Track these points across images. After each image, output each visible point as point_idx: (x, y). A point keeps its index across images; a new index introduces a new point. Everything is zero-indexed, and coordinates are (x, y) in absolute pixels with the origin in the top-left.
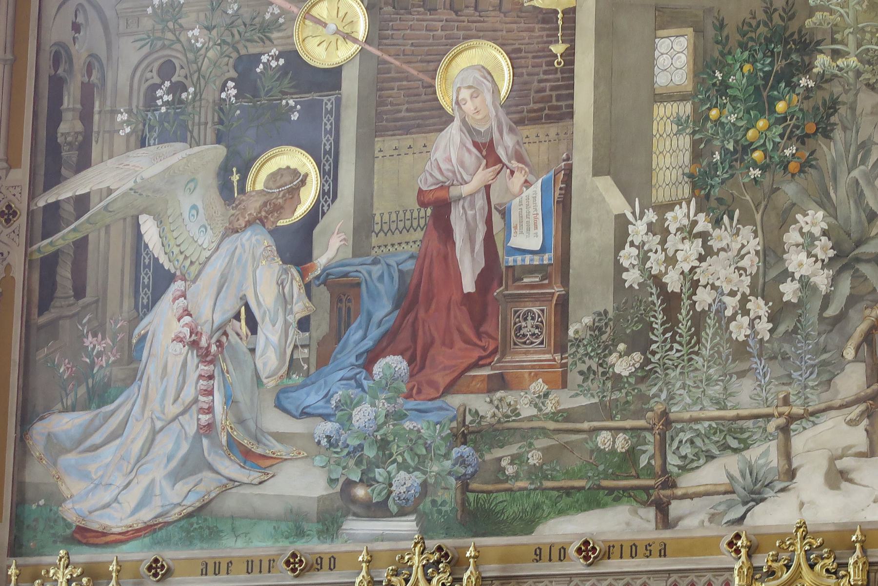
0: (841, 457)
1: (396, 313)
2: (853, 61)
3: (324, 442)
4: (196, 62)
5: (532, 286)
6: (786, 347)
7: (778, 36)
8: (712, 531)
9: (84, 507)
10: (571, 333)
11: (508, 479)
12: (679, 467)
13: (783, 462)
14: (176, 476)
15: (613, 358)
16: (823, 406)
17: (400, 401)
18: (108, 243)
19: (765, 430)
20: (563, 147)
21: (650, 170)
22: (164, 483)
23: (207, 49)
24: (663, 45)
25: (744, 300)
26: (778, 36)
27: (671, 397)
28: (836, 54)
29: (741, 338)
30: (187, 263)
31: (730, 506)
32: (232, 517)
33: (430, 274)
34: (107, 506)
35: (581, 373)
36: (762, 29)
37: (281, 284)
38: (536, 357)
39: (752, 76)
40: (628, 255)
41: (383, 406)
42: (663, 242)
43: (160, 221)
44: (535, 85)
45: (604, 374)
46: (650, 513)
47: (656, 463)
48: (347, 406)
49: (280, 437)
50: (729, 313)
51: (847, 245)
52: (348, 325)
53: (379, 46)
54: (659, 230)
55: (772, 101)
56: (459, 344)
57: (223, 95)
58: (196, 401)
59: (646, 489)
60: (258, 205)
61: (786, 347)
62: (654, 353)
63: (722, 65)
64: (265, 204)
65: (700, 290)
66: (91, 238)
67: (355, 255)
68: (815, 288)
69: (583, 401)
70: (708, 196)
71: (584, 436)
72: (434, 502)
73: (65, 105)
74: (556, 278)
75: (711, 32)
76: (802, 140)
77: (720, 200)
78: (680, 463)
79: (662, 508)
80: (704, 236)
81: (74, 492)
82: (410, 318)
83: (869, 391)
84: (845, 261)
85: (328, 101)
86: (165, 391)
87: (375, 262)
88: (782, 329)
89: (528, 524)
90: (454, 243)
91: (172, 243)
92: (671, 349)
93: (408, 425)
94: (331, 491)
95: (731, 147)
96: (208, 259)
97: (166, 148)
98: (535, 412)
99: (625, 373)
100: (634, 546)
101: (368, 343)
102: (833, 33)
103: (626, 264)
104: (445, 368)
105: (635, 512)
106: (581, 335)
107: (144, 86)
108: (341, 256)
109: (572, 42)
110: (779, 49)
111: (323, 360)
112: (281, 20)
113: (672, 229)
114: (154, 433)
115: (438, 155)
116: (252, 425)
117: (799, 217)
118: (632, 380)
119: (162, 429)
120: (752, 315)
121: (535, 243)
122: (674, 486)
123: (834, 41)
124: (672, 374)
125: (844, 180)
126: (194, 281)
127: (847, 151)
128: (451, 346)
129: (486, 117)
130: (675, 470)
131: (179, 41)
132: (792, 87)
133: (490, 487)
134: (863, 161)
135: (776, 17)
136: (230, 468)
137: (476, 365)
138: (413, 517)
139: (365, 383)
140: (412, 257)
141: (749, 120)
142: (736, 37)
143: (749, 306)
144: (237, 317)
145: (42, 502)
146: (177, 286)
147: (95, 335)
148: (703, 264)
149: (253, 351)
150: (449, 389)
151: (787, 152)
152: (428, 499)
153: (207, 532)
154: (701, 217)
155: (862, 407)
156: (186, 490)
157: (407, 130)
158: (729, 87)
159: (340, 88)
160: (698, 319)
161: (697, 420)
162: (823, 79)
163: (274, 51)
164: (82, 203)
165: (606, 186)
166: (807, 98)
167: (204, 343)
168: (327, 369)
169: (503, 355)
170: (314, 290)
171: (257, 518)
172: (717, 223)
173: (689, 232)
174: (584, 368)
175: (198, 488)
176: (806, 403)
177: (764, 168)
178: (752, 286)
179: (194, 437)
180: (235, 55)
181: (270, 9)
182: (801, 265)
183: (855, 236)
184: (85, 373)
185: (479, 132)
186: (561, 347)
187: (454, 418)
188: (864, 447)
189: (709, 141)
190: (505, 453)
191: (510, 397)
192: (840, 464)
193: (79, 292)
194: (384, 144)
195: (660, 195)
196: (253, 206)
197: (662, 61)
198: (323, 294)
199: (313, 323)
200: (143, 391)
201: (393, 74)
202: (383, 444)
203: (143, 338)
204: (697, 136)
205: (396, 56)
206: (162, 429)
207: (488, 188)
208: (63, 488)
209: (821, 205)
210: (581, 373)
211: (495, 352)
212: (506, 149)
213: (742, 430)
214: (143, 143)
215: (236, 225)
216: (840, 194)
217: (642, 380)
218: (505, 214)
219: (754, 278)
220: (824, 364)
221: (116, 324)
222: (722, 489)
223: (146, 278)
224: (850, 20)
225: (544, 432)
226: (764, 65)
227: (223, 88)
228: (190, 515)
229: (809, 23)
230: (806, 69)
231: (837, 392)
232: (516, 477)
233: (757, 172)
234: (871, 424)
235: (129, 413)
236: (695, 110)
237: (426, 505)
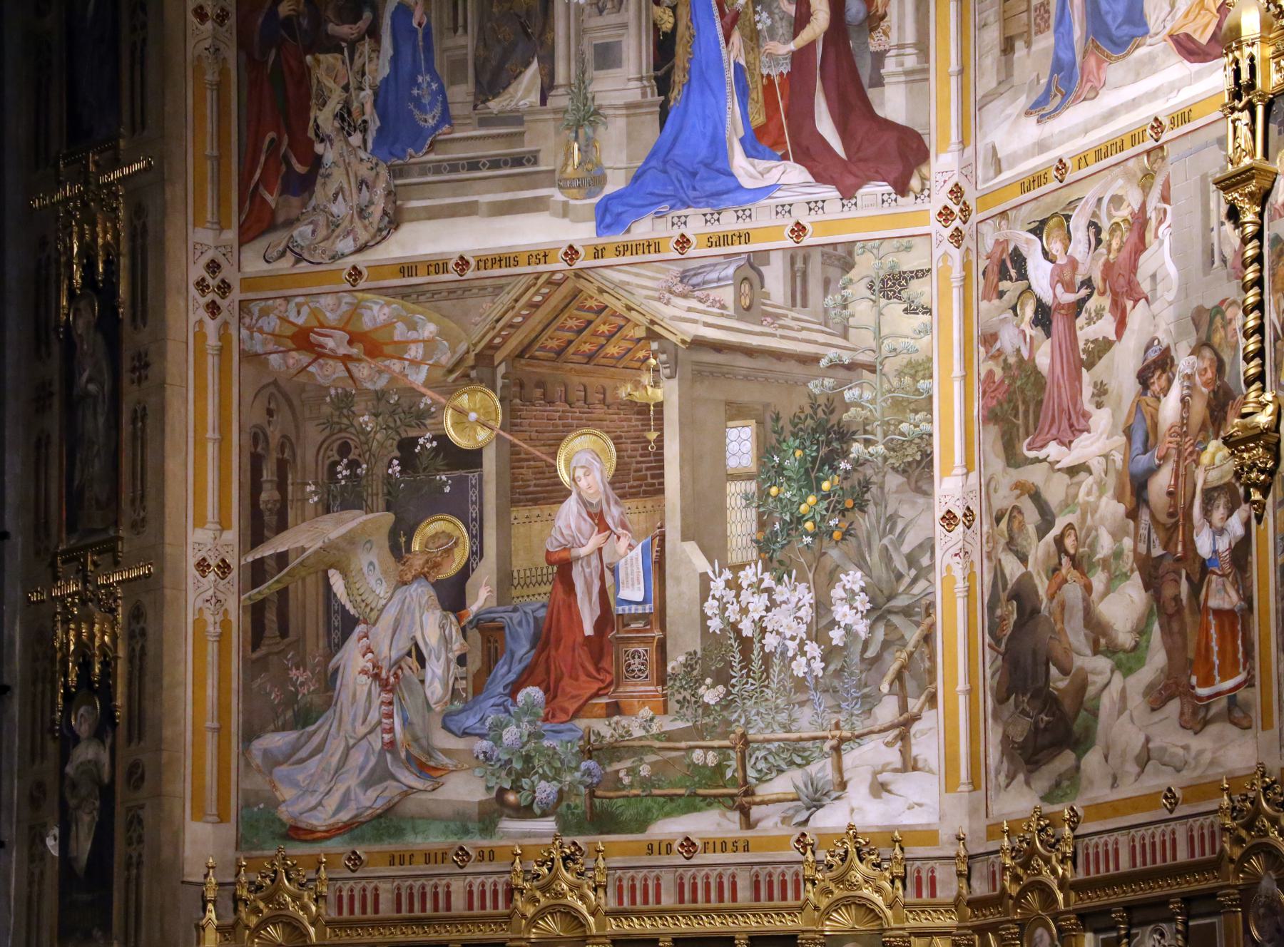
0: (881, 773)
1: (533, 652)
2: (880, 449)
3: (481, 757)
4: (366, 443)
5: (638, 631)
6: (836, 683)
7: (821, 427)
8: (784, 830)
9: (296, 809)
10: (669, 669)
11: (625, 787)
12: (757, 779)
13: (837, 776)
14: (367, 784)
15: (702, 690)
16: (866, 730)
17: (539, 723)
18: (304, 592)
19: (822, 750)
20: (657, 517)
21: (725, 537)
22: (358, 790)
23: (376, 433)
24: (732, 434)
25: (802, 644)
26: (821, 427)
27: (748, 722)
28: (868, 443)
29: (801, 675)
30: (368, 610)
31: (797, 811)
32: (412, 818)
33: (558, 620)
34: (314, 808)
35: (678, 702)
36: (809, 421)
37: (442, 627)
38: (643, 688)
39: (803, 461)
40: (711, 606)
41: (526, 728)
42: (737, 596)
43: (345, 576)
44: (634, 466)
45: (696, 702)
46: (736, 816)
47: (739, 775)
48: (499, 727)
49: (447, 752)
50: (790, 654)
51: (881, 600)
52: (496, 661)
53: (511, 432)
54: (734, 585)
55: (819, 481)
56: (583, 678)
57: (390, 471)
58: (380, 723)
59: (732, 796)
60: (421, 562)
61: (836, 683)
62: (733, 686)
63: (779, 451)
64: (427, 562)
65: (767, 635)
66: (291, 587)
67: (499, 605)
68: (856, 635)
69: (681, 725)
70: (771, 559)
71: (682, 753)
72: (568, 806)
73: (265, 477)
74: (656, 625)
75: (769, 423)
76: (843, 513)
77: (781, 562)
78: (755, 775)
79: (745, 812)
80: (769, 591)
81: (287, 797)
82: (544, 656)
83: (901, 719)
84: (879, 613)
85: (473, 477)
86: (355, 715)
87: (515, 610)
88: (832, 668)
89: (642, 824)
90: (575, 595)
91: (355, 592)
92: (747, 683)
93: (546, 743)
94: (488, 797)
95: (787, 518)
96: (385, 606)
97: (347, 514)
98: (643, 733)
99: (712, 702)
100: (724, 843)
101: (512, 677)
102: (865, 425)
103: (709, 613)
104: (573, 697)
105: (724, 815)
106: (677, 671)
107: (327, 462)
108: (488, 605)
109: (661, 430)
110: (823, 438)
111: (478, 689)
112: (433, 409)
113: (745, 585)
114: (348, 749)
115: (560, 523)
116: (424, 742)
117: (842, 576)
118: (718, 708)
119: (354, 745)
120: (809, 656)
121: (639, 596)
122: (753, 794)
123: (866, 432)
124: (749, 703)
125: (876, 546)
126: (374, 624)
127: (878, 522)
128: (577, 679)
129: (597, 492)
130: (754, 781)
131: (352, 425)
132: (834, 469)
133: (611, 794)
134: (892, 530)
135: (820, 411)
136: (409, 779)
137: (596, 695)
138: (553, 818)
139: (511, 709)
140: (543, 606)
141: (801, 497)
142: (789, 428)
143: (806, 648)
144: (409, 654)
145: (262, 806)
146: (360, 628)
147: (298, 669)
148: (770, 614)
149: (422, 682)
150: (576, 715)
151: (832, 523)
152: (564, 804)
153: (392, 831)
154: (767, 576)
155: (896, 732)
156: (375, 795)
157: (535, 502)
158: (784, 469)
159: (481, 466)
160: (767, 658)
161: (769, 741)
162: (858, 463)
163: (428, 435)
164: (282, 559)
165: (692, 549)
166: (846, 479)
167: (384, 675)
168: (482, 697)
169: (618, 686)
170: (469, 633)
171: (432, 818)
172: (779, 580)
173: (758, 588)
174: (680, 697)
175: (385, 794)
176: (852, 728)
177: (814, 536)
178: (808, 632)
179: (380, 753)
180: (397, 438)
181: (424, 400)
182: (845, 615)
183: (886, 592)
184: (291, 699)
185: (591, 504)
186: (662, 680)
187: (581, 738)
188: (899, 765)
189: (770, 514)
190: (622, 766)
191: (624, 721)
192: (881, 778)
193: (284, 632)
194: (519, 513)
195: (734, 558)
196: (418, 563)
197: (732, 447)
198: (475, 635)
199: (469, 660)
200: (337, 715)
201: (523, 456)
202: (528, 759)
203: (336, 670)
204: (761, 510)
205: (524, 440)
206: (354, 745)
207: (600, 550)
208: (278, 794)
209: (860, 568)
210: (678, 702)
211: (610, 684)
212: (613, 518)
213: (804, 750)
214: (328, 510)
215: (405, 578)
216: (874, 559)
217: (725, 707)
218: (615, 571)
219: (809, 626)
220: (865, 696)
221: (314, 658)
222: (790, 797)
223: (336, 622)
224: (878, 415)
225: (651, 749)
226: (811, 451)
227: (390, 465)
228: (379, 816)
229: (845, 417)
230: (845, 454)
231: (876, 719)
232: (631, 786)
233: (809, 539)
234: (903, 746)
235: (328, 732)
236: (759, 488)
237: (563, 808)
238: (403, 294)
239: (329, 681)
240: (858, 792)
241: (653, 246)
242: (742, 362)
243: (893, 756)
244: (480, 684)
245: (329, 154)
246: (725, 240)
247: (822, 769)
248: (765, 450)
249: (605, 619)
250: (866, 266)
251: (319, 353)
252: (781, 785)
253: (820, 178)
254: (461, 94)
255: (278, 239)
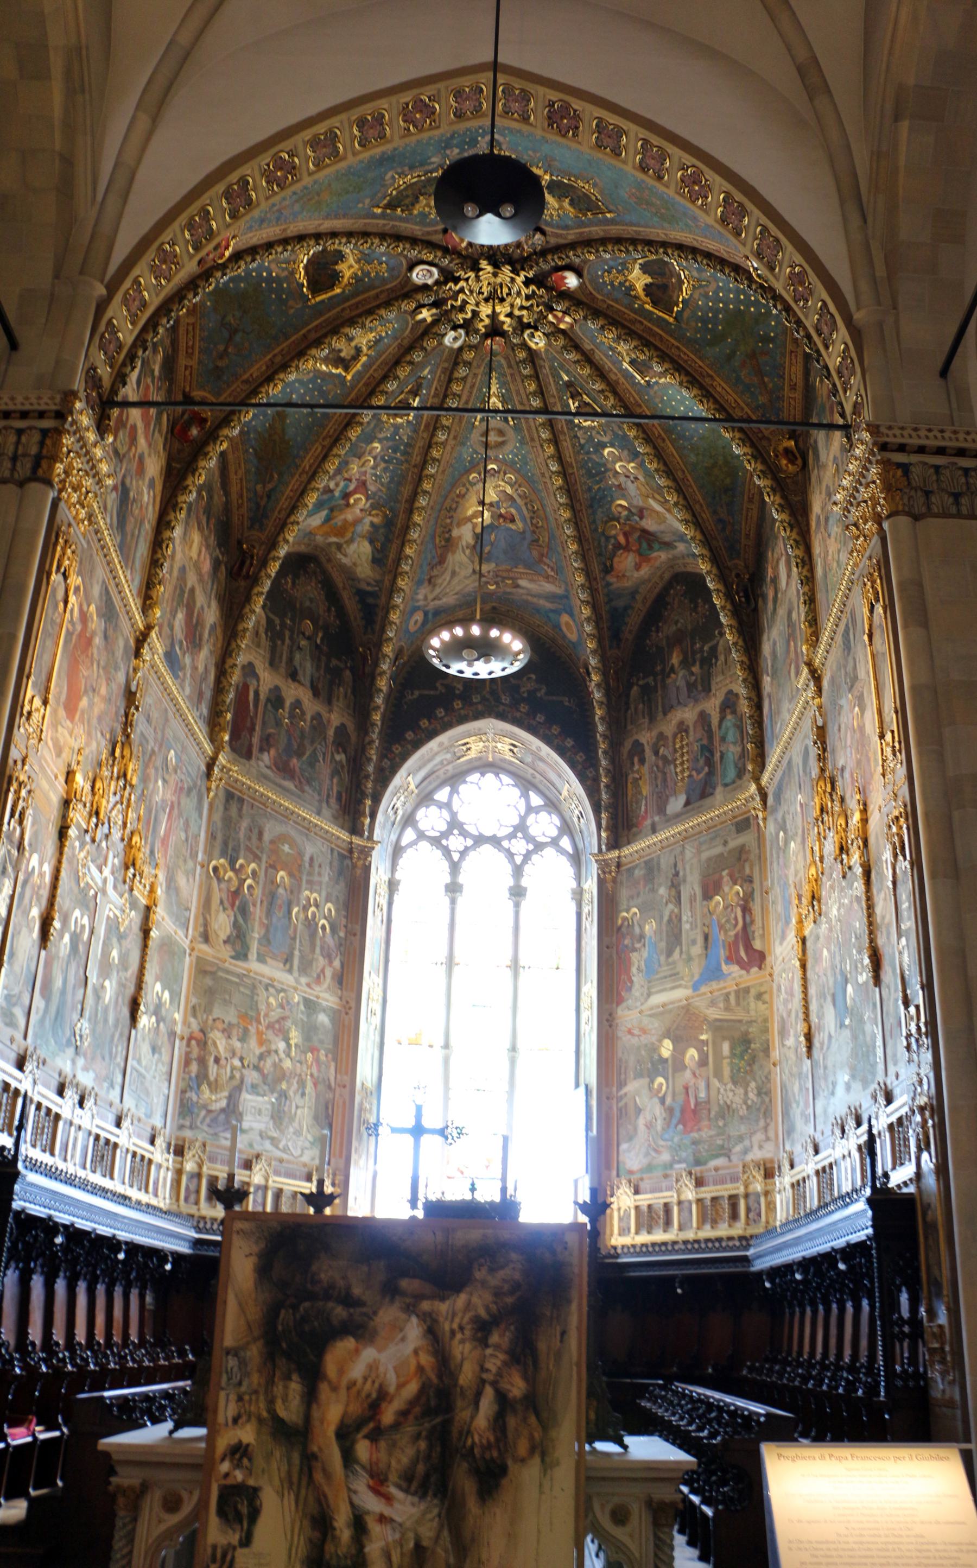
89: (705, 1163)
186: (709, 1119)
238: (650, 1016)
239: (635, 1129)
240: (756, 1148)
241: (704, 994)
242: (725, 1024)
243: (763, 1137)
244: (668, 1126)
245: (634, 979)
246: (720, 989)
247: (747, 1143)
248: (732, 1048)
249: (697, 1104)
250: (753, 992)
251: (633, 1034)
252: (738, 1148)
253: (742, 968)
254: (663, 958)
255: (624, 1005)
